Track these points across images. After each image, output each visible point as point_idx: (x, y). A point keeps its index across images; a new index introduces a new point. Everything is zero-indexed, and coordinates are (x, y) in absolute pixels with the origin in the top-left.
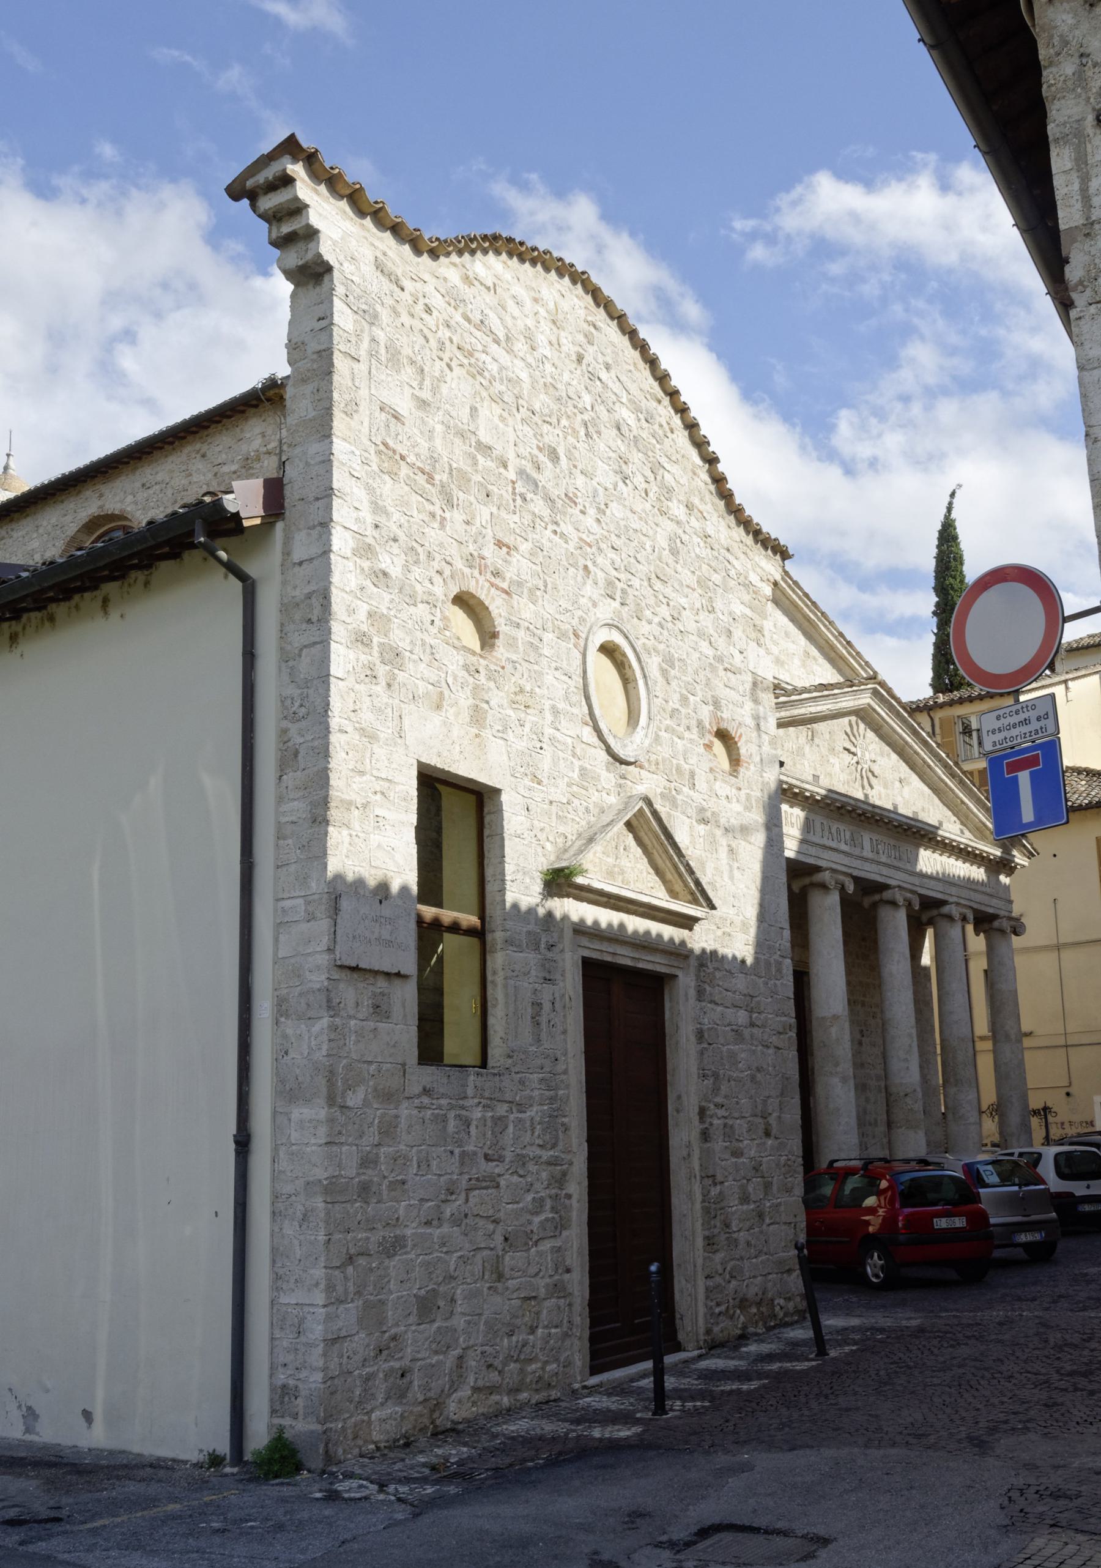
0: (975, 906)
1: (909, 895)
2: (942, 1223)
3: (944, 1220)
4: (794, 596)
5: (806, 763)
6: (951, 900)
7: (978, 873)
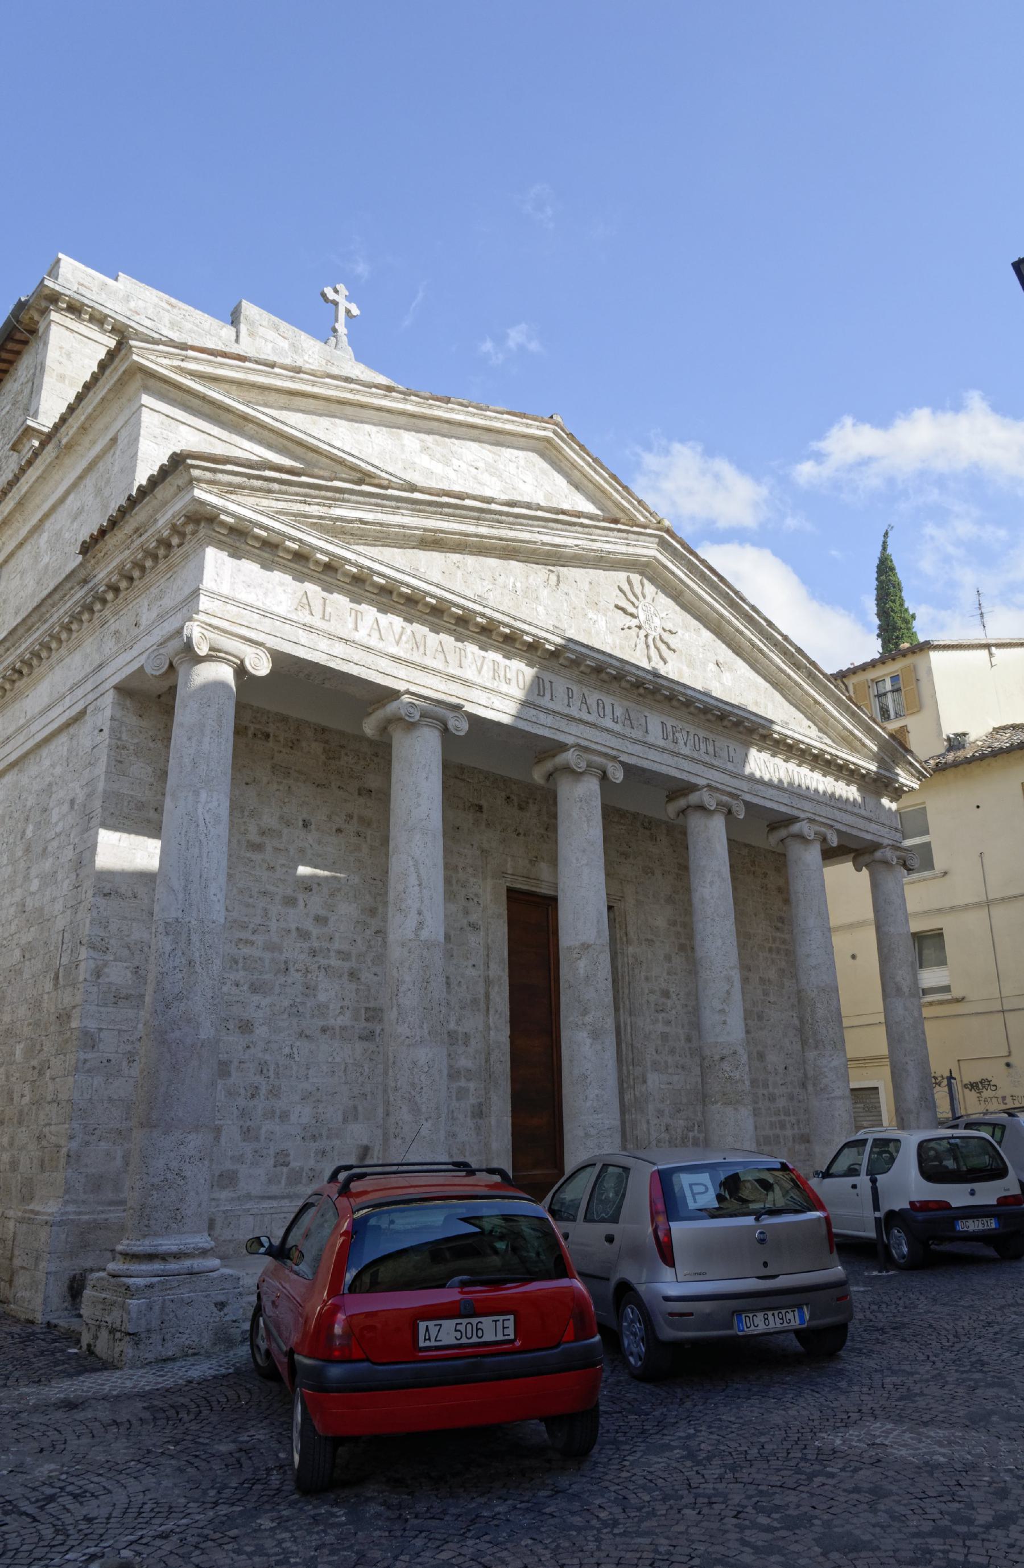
0: (843, 828)
1: (725, 798)
2: (442, 1333)
3: (448, 1324)
4: (597, 478)
5: (541, 609)
6: (802, 815)
7: (850, 792)
